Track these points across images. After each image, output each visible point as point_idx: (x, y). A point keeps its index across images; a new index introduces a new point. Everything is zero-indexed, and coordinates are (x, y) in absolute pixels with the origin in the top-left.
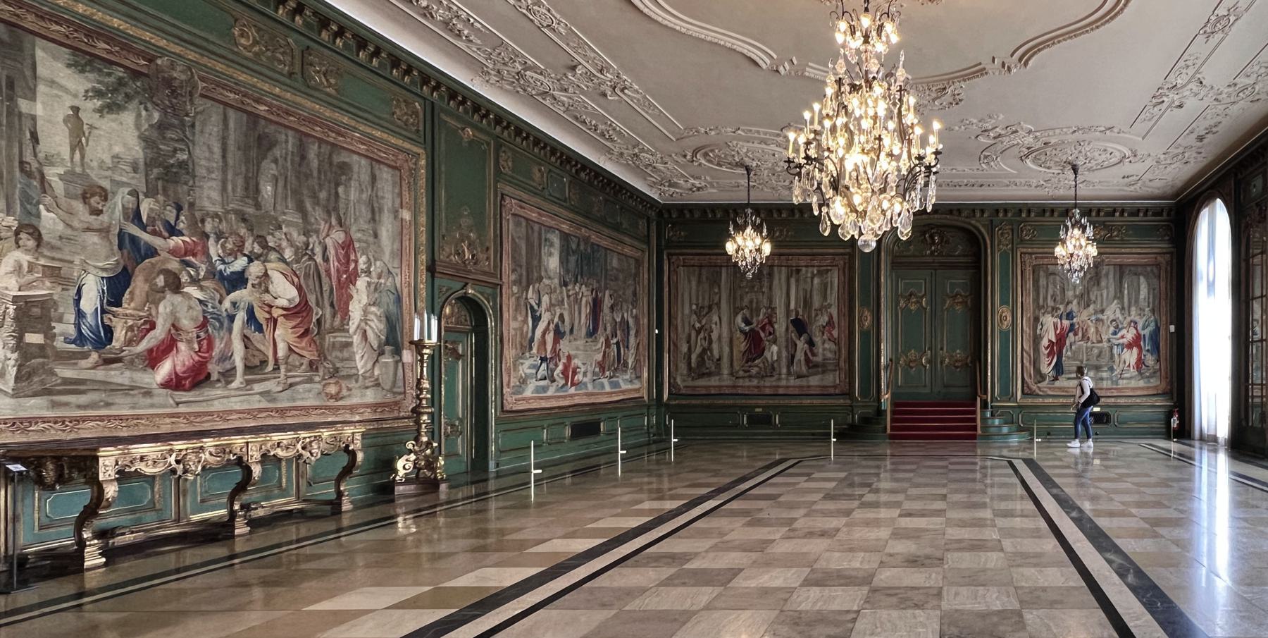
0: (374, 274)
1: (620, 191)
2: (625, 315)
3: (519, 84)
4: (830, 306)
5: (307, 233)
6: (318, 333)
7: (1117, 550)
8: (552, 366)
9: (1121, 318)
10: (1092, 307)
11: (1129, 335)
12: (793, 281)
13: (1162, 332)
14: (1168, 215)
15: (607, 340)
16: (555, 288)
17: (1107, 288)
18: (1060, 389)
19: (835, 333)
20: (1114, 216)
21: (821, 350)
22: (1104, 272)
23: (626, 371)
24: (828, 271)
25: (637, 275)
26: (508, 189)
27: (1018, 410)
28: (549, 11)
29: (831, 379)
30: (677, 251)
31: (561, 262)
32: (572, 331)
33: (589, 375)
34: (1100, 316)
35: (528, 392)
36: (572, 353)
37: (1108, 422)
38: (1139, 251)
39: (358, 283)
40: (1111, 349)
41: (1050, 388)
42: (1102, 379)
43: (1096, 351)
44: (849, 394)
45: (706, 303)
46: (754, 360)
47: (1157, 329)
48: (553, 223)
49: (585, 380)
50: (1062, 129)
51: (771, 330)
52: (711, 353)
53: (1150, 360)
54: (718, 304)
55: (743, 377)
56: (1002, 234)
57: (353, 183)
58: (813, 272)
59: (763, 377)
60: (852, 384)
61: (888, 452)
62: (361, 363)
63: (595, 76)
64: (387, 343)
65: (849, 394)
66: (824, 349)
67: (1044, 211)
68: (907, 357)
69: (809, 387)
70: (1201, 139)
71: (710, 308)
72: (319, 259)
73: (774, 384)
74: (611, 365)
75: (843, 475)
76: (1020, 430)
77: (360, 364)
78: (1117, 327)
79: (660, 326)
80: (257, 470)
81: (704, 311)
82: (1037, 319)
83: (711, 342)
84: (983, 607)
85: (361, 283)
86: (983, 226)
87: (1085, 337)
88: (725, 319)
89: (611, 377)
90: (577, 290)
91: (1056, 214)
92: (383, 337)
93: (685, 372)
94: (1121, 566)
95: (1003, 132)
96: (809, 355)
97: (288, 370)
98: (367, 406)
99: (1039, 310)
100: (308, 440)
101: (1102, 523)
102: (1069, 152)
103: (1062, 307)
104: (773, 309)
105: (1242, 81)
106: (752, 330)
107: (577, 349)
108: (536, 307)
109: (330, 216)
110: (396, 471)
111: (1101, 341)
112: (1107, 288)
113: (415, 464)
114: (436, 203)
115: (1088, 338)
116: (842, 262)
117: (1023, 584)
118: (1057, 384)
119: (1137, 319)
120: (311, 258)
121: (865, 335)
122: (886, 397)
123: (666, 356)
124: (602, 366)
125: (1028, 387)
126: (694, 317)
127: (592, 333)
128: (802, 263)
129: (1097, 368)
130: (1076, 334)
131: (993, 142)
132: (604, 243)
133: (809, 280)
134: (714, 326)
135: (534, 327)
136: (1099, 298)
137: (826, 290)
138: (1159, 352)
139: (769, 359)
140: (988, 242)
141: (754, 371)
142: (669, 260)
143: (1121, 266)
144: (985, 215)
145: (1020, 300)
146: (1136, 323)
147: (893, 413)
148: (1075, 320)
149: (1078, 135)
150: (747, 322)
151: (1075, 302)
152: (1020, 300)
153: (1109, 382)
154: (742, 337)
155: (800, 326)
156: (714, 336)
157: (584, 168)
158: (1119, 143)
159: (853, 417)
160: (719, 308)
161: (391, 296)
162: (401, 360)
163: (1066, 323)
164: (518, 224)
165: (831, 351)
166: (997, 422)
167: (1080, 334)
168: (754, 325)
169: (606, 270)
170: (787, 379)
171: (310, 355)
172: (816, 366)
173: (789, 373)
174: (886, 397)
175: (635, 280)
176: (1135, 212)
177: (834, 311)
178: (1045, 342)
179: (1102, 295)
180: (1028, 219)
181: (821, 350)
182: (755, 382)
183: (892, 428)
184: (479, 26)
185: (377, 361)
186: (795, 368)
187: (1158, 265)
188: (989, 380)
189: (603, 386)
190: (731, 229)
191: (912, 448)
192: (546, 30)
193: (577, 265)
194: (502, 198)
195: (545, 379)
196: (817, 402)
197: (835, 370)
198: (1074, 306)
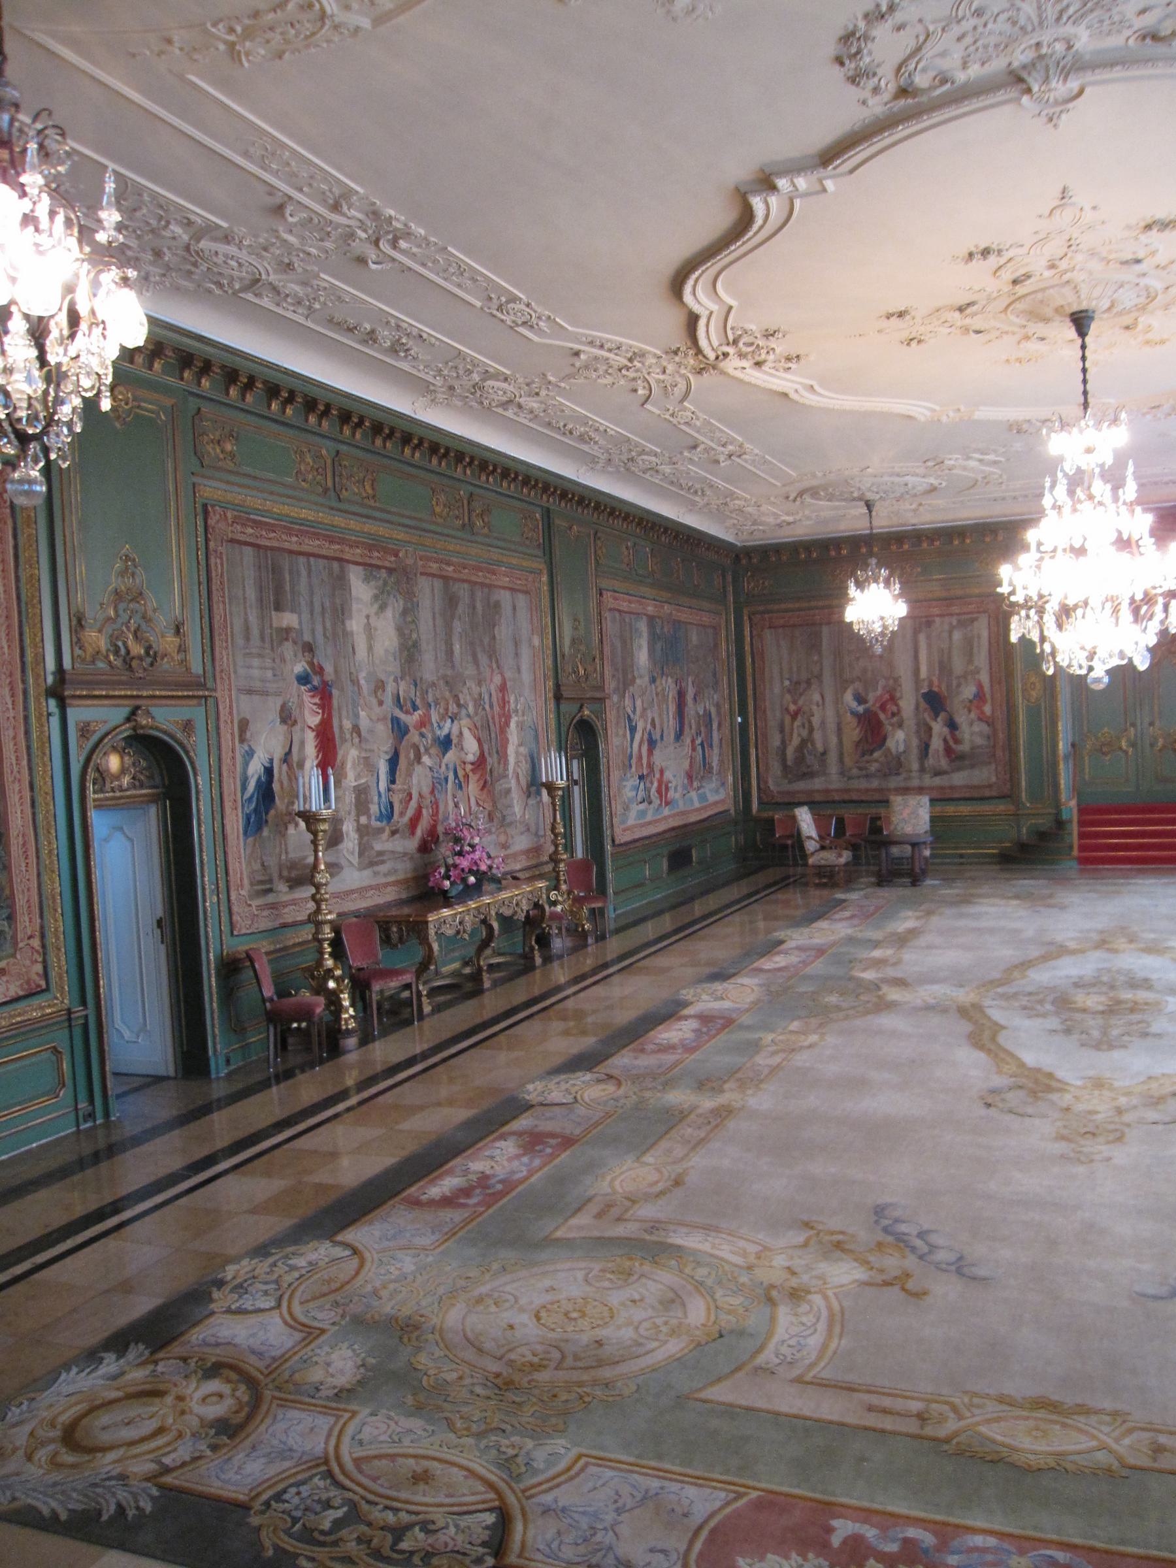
1: (698, 544)
4: (977, 671)
19: (987, 709)
21: (967, 736)
24: (973, 620)
25: (716, 646)
29: (983, 775)
30: (761, 608)
33: (680, 789)
44: (1010, 796)
46: (872, 752)
51: (895, 709)
52: (813, 744)
54: (819, 677)
55: (859, 777)
58: (951, 624)
59: (885, 775)
60: (1014, 780)
66: (972, 734)
73: (902, 784)
79: (743, 712)
81: (798, 688)
83: (811, 730)
88: (829, 698)
89: (699, 788)
96: (951, 743)
104: (896, 680)
106: (867, 711)
123: (753, 751)
126: (788, 697)
132: (684, 616)
133: (945, 635)
134: (814, 708)
137: (972, 649)
139: (894, 751)
141: (874, 767)
142: (750, 619)
147: (1081, 823)
150: (860, 700)
154: (853, 722)
155: (934, 701)
156: (816, 721)
157: (666, 530)
159: (1019, 831)
160: (821, 682)
170: (920, 778)
172: (961, 757)
173: (922, 770)
177: (984, 678)
182: (875, 784)
183: (1082, 848)
186: (930, 761)
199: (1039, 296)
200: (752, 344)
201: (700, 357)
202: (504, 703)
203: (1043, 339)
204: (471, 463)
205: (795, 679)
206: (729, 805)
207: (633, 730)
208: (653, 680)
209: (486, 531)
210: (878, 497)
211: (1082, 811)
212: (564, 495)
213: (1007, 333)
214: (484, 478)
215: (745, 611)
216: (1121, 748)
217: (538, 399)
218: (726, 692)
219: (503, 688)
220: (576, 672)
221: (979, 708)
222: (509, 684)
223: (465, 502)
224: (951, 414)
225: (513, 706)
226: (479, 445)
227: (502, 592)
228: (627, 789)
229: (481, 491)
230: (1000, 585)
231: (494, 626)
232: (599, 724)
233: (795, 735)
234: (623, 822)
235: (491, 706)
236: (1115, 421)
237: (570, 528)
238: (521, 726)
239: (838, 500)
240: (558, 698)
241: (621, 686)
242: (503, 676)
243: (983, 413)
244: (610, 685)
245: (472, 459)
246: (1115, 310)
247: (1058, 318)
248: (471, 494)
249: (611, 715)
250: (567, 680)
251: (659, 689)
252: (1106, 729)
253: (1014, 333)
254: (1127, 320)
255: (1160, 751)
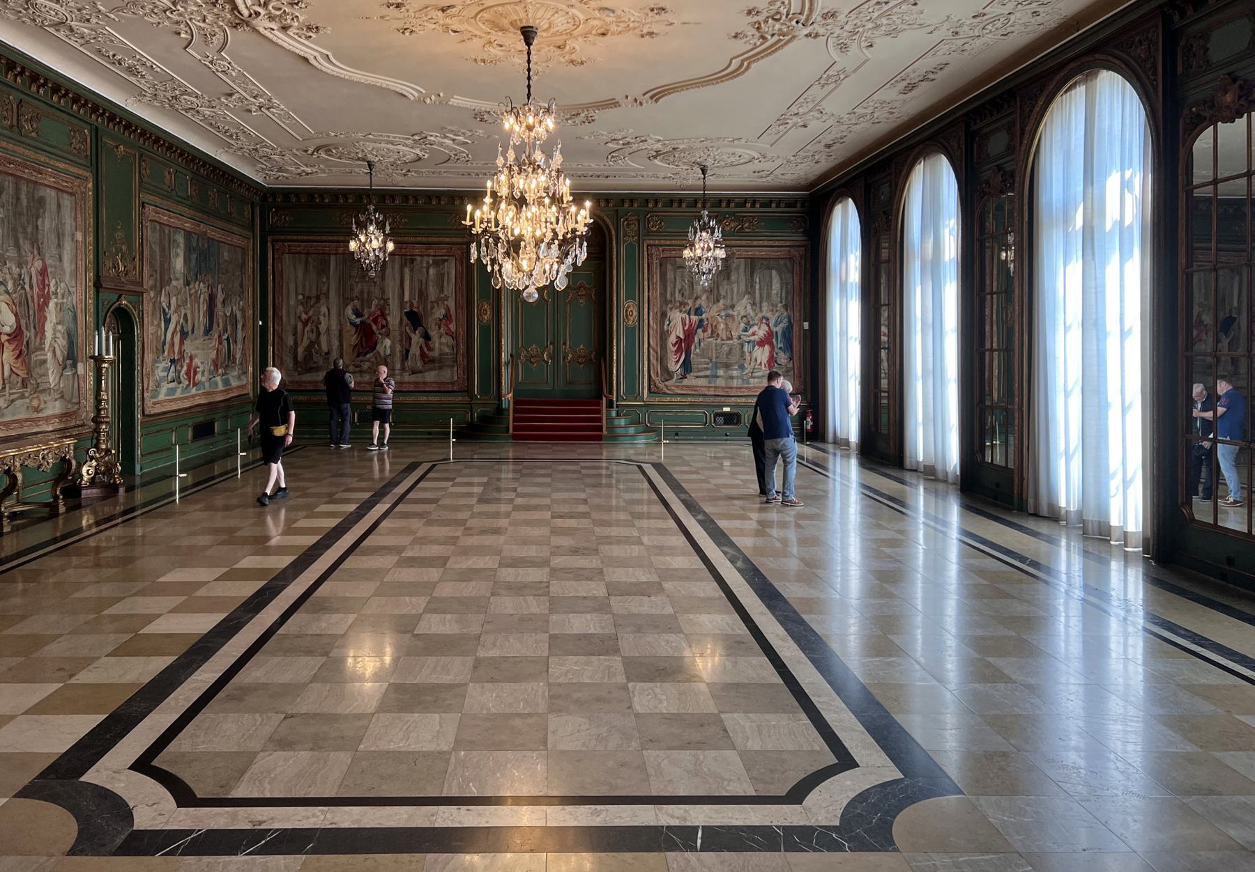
0: (60, 296)
1: (232, 181)
2: (234, 308)
3: (172, 106)
4: (447, 298)
5: (20, 266)
6: (27, 354)
7: (732, 545)
8: (178, 368)
9: (752, 314)
10: (721, 301)
11: (761, 332)
12: (407, 270)
13: (796, 328)
14: (802, 206)
15: (220, 336)
16: (181, 288)
17: (738, 283)
18: (688, 387)
19: (453, 327)
20: (745, 207)
21: (437, 345)
22: (734, 266)
23: (234, 367)
24: (444, 261)
25: (243, 265)
26: (147, 198)
27: (644, 409)
28: (230, 63)
29: (448, 375)
30: (283, 237)
31: (185, 262)
32: (193, 332)
34: (730, 312)
35: (162, 397)
36: (193, 352)
37: (738, 422)
38: (771, 243)
39: (50, 304)
40: (742, 346)
41: (678, 387)
42: (732, 378)
43: (726, 348)
44: (468, 390)
45: (314, 293)
47: (790, 327)
48: (175, 222)
49: (204, 379)
50: (690, 139)
52: (320, 348)
53: (783, 358)
54: (327, 295)
56: (628, 224)
57: (46, 215)
61: (511, 454)
62: (52, 378)
63: (247, 99)
64: (68, 358)
65: (467, 391)
66: (441, 344)
67: (672, 201)
68: (528, 351)
69: (424, 383)
70: (828, 146)
71: (318, 298)
72: (27, 287)
74: (223, 362)
75: (485, 480)
76: (647, 430)
77: (51, 380)
78: (748, 323)
79: (264, 317)
80: (19, 476)
82: (664, 315)
83: (319, 334)
84: (633, 580)
85: (52, 304)
86: (608, 216)
87: (714, 334)
89: (223, 375)
90: (197, 286)
91: (684, 205)
92: (66, 353)
93: (291, 365)
94: (733, 556)
95: (632, 141)
96: (425, 349)
97: (11, 389)
98: (55, 416)
99: (667, 305)
100: (46, 452)
101: (723, 524)
102: (698, 155)
103: (690, 302)
104: (386, 301)
105: (859, 111)
106: (362, 322)
107: (198, 349)
108: (167, 309)
109: (33, 247)
110: (81, 476)
111: (730, 338)
112: (738, 283)
113: (96, 469)
114: (100, 219)
115: (718, 335)
116: (459, 252)
117: (661, 567)
118: (685, 382)
119: (768, 315)
120: (23, 288)
121: (485, 330)
122: (508, 397)
123: (270, 349)
124: (215, 364)
125: (655, 385)
126: (301, 308)
127: (208, 331)
128: (417, 252)
129: (727, 366)
130: (704, 331)
131: (622, 147)
132: (217, 236)
133: (425, 270)
134: (322, 318)
135: (166, 329)
136: (729, 292)
138: (792, 351)
139: (382, 354)
140: (613, 232)
143: (751, 258)
144: (611, 205)
145: (646, 294)
146: (767, 319)
147: (515, 411)
148: (704, 316)
149: (708, 143)
150: (358, 314)
151: (704, 297)
152: (646, 294)
153: (740, 381)
154: (353, 330)
155: (414, 319)
156: (323, 327)
158: (746, 148)
161: (70, 313)
162: (76, 372)
163: (695, 318)
164: (154, 230)
165: (448, 346)
166: (622, 422)
167: (709, 331)
168: (366, 316)
169: (219, 264)
170: (401, 375)
171: (22, 374)
172: (432, 361)
173: (403, 369)
174: (508, 397)
175: (241, 271)
176: (767, 203)
177: (451, 303)
178: (672, 339)
179: (732, 289)
180: (655, 209)
181: (437, 345)
183: (515, 428)
184: (159, 70)
185: (62, 375)
186: (409, 363)
187: (791, 259)
188: (615, 378)
189: (216, 384)
190: (354, 226)
191: (540, 451)
192: (219, 74)
193: (196, 263)
194: (143, 207)
195: (174, 381)
196: (434, 399)
197: (453, 366)
198: (703, 301)
199: (500, 9)
200: (280, 9)
201: (236, 12)
202: (43, 285)
203: (501, 46)
204: (22, 73)
205: (307, 294)
206: (249, 390)
207: (167, 322)
208: (187, 283)
209: (33, 134)
210: (377, 159)
211: (516, 402)
212: (112, 118)
213: (476, 36)
214: (34, 88)
215: (269, 239)
216: (544, 360)
217: (87, 25)
218: (251, 300)
219: (43, 272)
220: (115, 266)
221: (447, 326)
222: (49, 270)
223: (15, 106)
224: (433, 98)
225: (52, 289)
226: (31, 59)
227: (48, 190)
228: (160, 369)
229: (29, 99)
230: (465, 220)
231: (38, 218)
232: (136, 313)
233: (305, 338)
234: (155, 394)
235: (31, 287)
236: (548, 111)
237: (117, 147)
238: (60, 307)
239: (346, 158)
240: (98, 285)
241: (158, 284)
242: (43, 260)
243: (456, 101)
244: (148, 282)
245: (23, 69)
246: (552, 31)
247: (512, 29)
248: (21, 101)
249: (148, 307)
250: (108, 272)
251: (192, 291)
252: (534, 346)
253: (481, 38)
254: (559, 40)
255: (569, 362)
